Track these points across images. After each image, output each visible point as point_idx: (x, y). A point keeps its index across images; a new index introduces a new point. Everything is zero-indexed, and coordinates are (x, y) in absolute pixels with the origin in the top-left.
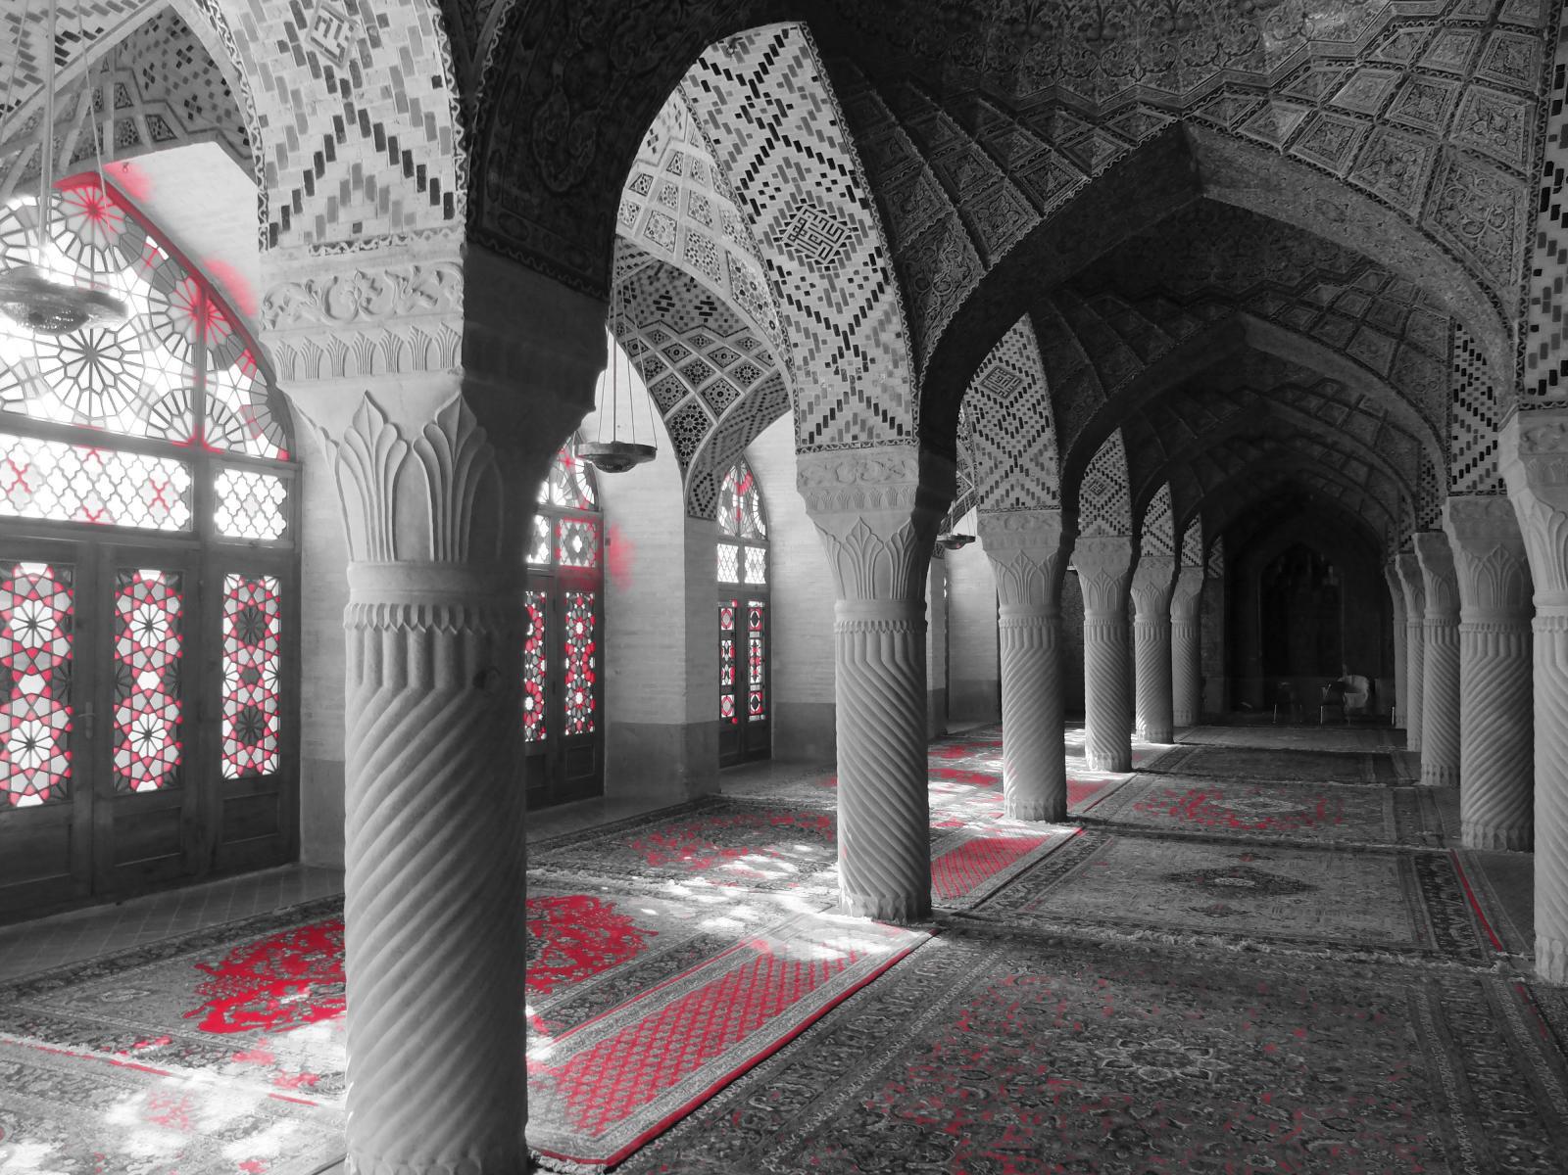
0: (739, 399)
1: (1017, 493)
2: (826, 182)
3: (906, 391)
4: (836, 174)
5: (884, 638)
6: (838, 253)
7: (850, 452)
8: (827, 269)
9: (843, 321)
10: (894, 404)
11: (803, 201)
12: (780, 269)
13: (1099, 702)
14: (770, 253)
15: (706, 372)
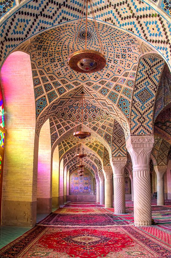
0: (65, 133)
1: (119, 154)
2: (152, 87)
3: (151, 126)
4: (154, 86)
5: (147, 172)
6: (147, 100)
7: (141, 136)
8: (143, 102)
9: (142, 112)
10: (149, 128)
11: (146, 89)
12: (135, 101)
13: (108, 195)
14: (134, 97)
15: (61, 127)
